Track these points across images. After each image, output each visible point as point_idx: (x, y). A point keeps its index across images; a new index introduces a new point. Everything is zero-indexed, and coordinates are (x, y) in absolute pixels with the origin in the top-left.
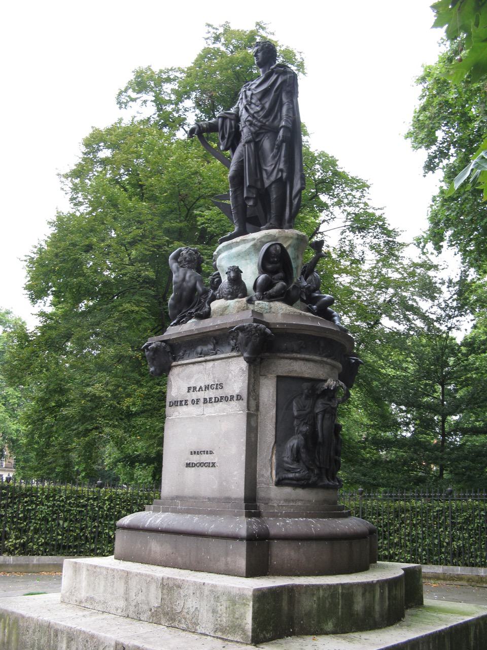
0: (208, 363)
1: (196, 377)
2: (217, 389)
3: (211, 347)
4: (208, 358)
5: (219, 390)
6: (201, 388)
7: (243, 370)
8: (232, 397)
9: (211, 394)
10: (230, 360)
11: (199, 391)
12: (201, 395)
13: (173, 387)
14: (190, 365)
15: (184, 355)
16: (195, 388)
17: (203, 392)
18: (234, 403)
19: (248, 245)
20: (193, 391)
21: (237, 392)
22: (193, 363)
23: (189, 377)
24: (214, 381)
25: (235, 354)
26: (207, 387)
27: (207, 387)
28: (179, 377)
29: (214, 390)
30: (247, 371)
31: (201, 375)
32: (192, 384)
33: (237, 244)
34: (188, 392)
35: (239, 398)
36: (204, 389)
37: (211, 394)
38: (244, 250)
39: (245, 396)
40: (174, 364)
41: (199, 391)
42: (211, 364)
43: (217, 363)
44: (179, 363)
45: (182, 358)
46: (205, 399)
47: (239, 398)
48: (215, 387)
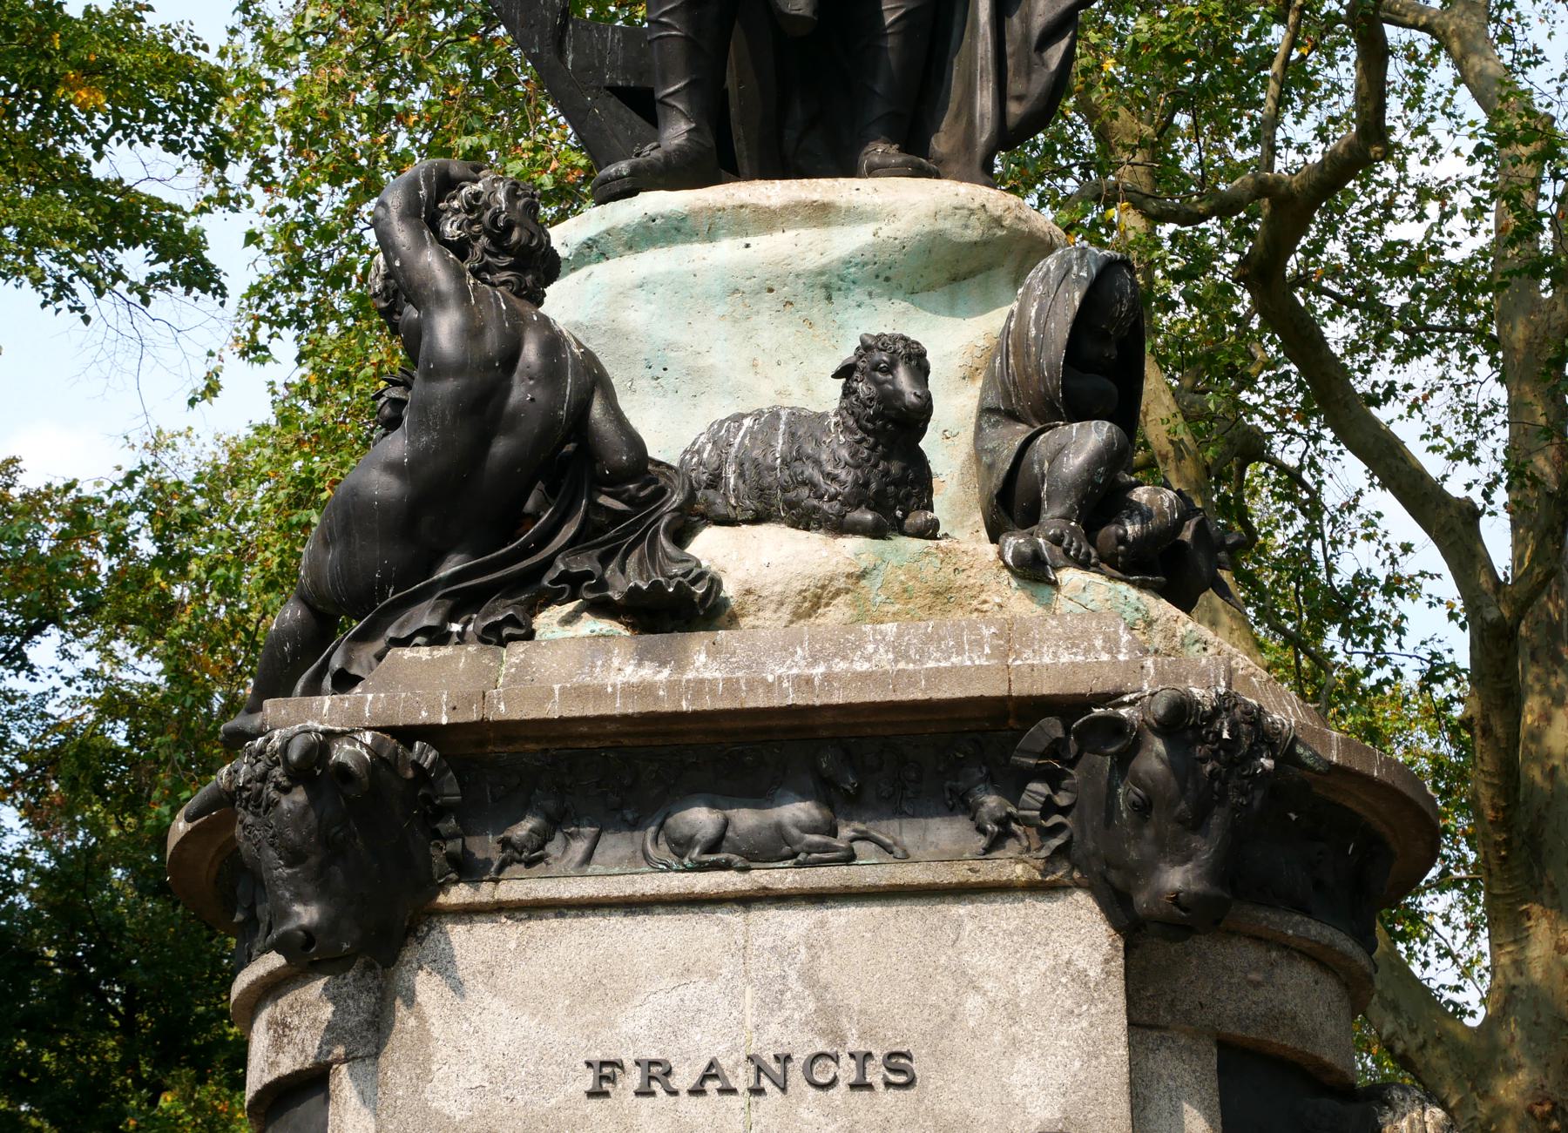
2: (860, 1085)
3: (796, 812)
4: (783, 877)
6: (711, 1072)
7: (1081, 978)
10: (961, 910)
11: (697, 1091)
13: (442, 1052)
15: (542, 838)
16: (656, 1074)
28: (495, 991)
30: (1118, 984)
33: (768, 220)
36: (742, 1078)
38: (813, 261)
40: (458, 894)
41: (697, 1091)
42: (796, 922)
43: (841, 917)
44: (514, 888)
45: (532, 857)
48: (847, 1070)
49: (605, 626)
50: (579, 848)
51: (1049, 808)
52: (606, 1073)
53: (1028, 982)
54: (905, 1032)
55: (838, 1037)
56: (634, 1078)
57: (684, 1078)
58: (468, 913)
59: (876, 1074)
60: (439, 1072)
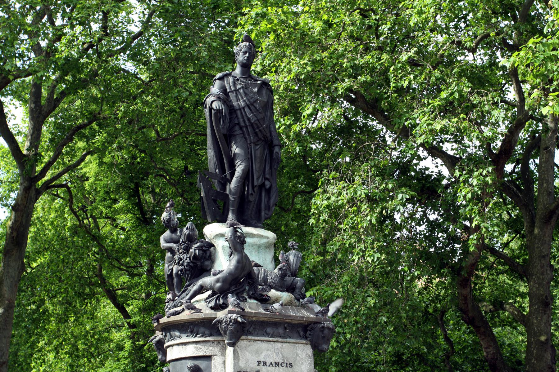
0: (276, 344)
1: (265, 353)
2: (287, 367)
4: (280, 340)
5: (289, 368)
6: (271, 363)
10: (297, 345)
11: (269, 366)
13: (241, 358)
14: (258, 342)
16: (265, 363)
17: (274, 368)
19: (264, 241)
20: (263, 365)
22: (262, 341)
23: (258, 352)
24: (284, 360)
25: (304, 342)
29: (284, 368)
31: (269, 352)
34: (258, 365)
36: (274, 365)
38: (258, 243)
41: (269, 366)
42: (279, 345)
43: (285, 345)
44: (250, 337)
45: (250, 334)
49: (256, 302)
50: (256, 333)
51: (310, 335)
52: (259, 363)
53: (304, 356)
54: (291, 361)
55: (284, 360)
56: (262, 364)
57: (268, 364)
58: (242, 340)
59: (288, 366)
60: (240, 361)
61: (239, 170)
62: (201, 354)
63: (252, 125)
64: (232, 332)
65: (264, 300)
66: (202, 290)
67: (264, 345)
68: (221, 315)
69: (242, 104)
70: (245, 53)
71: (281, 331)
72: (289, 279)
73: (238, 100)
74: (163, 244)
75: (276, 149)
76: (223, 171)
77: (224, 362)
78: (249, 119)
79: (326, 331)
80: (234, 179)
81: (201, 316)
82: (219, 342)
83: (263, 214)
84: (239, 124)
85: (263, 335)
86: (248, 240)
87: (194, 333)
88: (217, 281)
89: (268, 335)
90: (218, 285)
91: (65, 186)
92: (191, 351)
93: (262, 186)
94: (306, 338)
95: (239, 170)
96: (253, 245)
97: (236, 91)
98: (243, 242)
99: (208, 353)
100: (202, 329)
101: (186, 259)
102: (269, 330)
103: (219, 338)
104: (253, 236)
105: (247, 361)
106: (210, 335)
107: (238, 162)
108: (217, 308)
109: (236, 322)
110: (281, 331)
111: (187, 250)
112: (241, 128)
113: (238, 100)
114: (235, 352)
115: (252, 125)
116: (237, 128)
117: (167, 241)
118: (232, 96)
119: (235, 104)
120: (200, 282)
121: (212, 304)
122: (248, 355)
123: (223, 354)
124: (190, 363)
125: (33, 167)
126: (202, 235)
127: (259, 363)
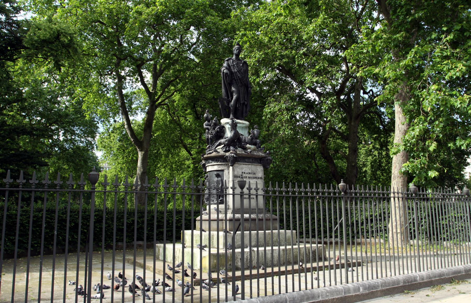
1: (245, 169)
8: (259, 178)
9: (251, 175)
12: (248, 175)
16: (245, 173)
18: (259, 180)
19: (245, 125)
21: (260, 176)
23: (242, 169)
26: (249, 173)
27: (249, 173)
32: (243, 171)
35: (261, 178)
37: (251, 175)
39: (263, 178)
42: (250, 166)
45: (239, 162)
46: (249, 177)
47: (261, 178)
52: (242, 173)
54: (255, 172)
61: (235, 97)
62: (220, 169)
63: (240, 79)
64: (232, 161)
65: (245, 149)
66: (220, 144)
67: (244, 166)
68: (227, 154)
69: (236, 71)
70: (237, 50)
71: (251, 160)
72: (254, 140)
73: (234, 69)
74: (205, 126)
75: (250, 89)
76: (228, 97)
77: (229, 172)
78: (239, 77)
79: (269, 161)
80: (233, 101)
81: (220, 154)
82: (227, 165)
83: (244, 114)
84: (234, 79)
85: (244, 162)
86: (238, 125)
87: (217, 161)
88: (226, 141)
89: (246, 162)
90: (226, 142)
91: (167, 104)
92: (216, 168)
93: (244, 103)
94: (261, 163)
95: (235, 97)
96: (240, 127)
97: (234, 65)
98: (236, 126)
99: (223, 169)
100: (220, 160)
101: (214, 132)
102: (246, 160)
103: (227, 163)
104: (240, 123)
105: (238, 172)
106: (223, 162)
107: (234, 94)
108: (226, 151)
109: (233, 156)
110: (251, 160)
111: (214, 129)
112: (235, 80)
113: (234, 69)
114: (233, 169)
115: (240, 79)
116: (234, 80)
117: (206, 125)
118: (232, 68)
119: (233, 70)
120: (219, 141)
121: (224, 150)
122: (238, 170)
123: (228, 169)
124: (215, 173)
125: (154, 97)
126: (220, 123)
127: (242, 173)
